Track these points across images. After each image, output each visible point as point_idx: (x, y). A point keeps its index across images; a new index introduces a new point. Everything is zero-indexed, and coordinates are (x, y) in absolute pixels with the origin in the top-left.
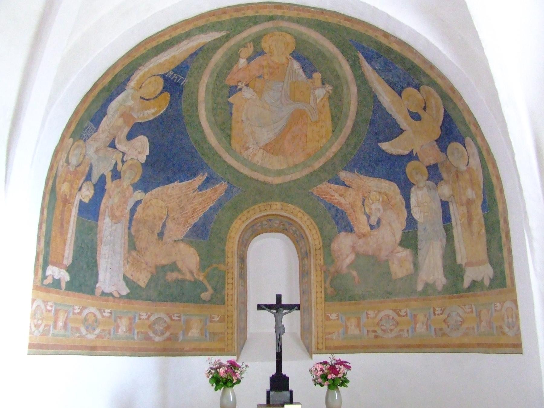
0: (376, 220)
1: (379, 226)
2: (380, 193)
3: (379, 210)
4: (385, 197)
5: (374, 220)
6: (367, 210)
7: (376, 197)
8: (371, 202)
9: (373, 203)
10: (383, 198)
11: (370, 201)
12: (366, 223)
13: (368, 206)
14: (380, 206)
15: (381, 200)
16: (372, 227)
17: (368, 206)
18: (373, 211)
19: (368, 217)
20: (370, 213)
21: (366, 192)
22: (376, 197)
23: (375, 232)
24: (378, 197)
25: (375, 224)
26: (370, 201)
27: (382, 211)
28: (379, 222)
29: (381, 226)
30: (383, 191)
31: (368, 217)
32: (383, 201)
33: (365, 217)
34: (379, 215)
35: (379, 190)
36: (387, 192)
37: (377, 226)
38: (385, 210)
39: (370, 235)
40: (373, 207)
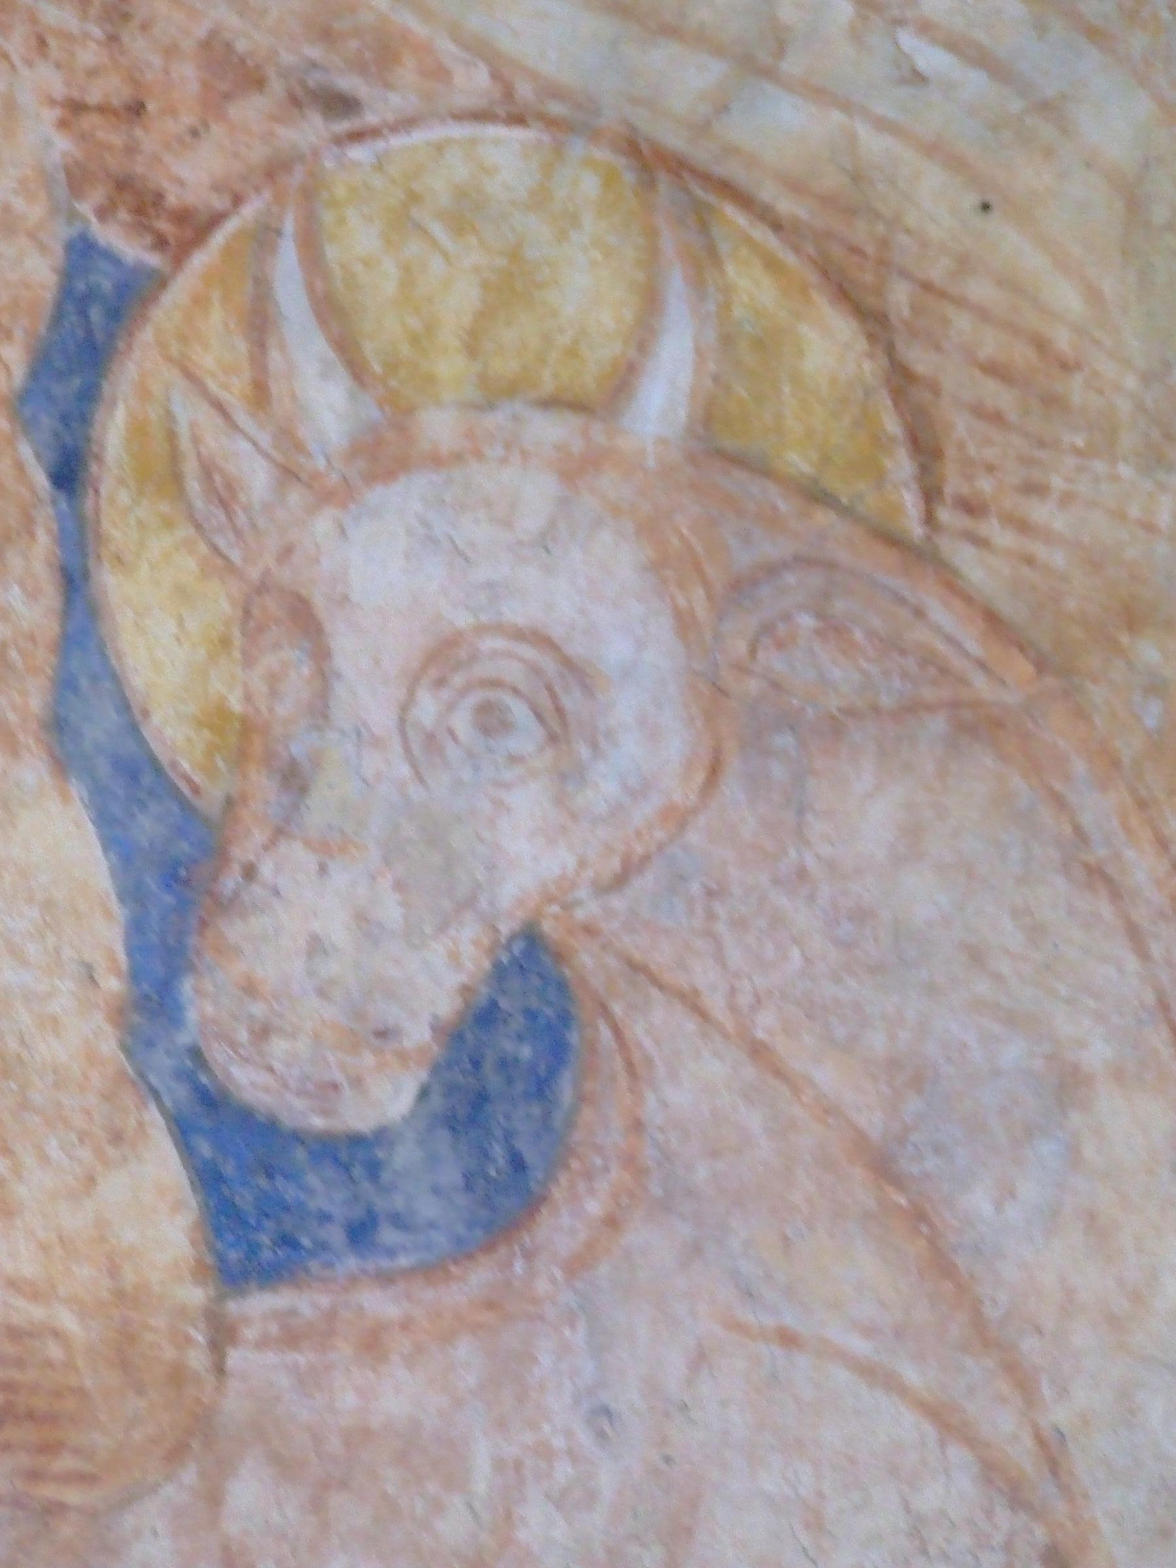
0: (435, 981)
1: (505, 1202)
2: (677, 183)
3: (559, 698)
4: (829, 347)
5: (341, 980)
6: (166, 643)
7: (513, 285)
8: (328, 406)
9: (384, 453)
10: (745, 354)
11: (304, 350)
12: (74, 1034)
13: (164, 469)
14: (602, 599)
15: (661, 405)
16: (264, 1195)
17: (164, 469)
18: (367, 686)
19: (178, 878)
20: (240, 736)
21: (232, 72)
22: (513, 285)
23: (373, 1363)
24: (587, 291)
25: (388, 1098)
26: (304, 350)
27: (645, 738)
28: (519, 1056)
29: (561, 1227)
30: (780, 130)
31: (178, 878)
32: (718, 444)
33: (61, 839)
34: (528, 853)
35: (680, 83)
36: (932, 204)
37: (427, 1184)
38: (745, 725)
39: (196, 1438)
40: (384, 571)
